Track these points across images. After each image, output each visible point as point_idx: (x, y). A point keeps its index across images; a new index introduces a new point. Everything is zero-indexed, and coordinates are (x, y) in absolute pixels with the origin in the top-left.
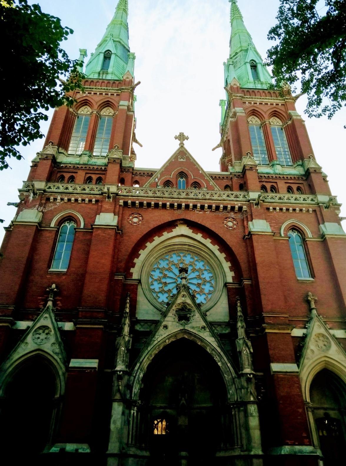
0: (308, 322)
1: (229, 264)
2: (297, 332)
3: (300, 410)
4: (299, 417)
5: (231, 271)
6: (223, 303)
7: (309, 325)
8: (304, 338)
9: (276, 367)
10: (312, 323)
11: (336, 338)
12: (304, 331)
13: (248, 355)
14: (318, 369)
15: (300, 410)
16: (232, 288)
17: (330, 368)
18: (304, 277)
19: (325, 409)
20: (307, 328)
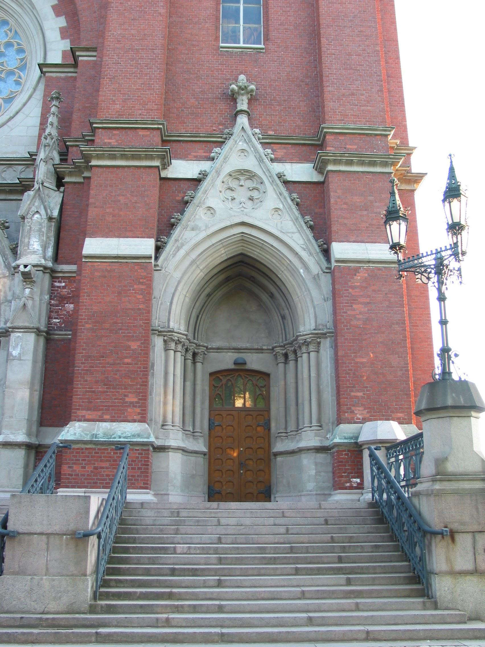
0: (221, 144)
1: (62, 22)
2: (182, 169)
3: (134, 345)
4: (126, 360)
5: (63, 38)
6: (31, 115)
7: (217, 150)
8: (196, 182)
9: (93, 246)
10: (230, 143)
11: (286, 183)
12: (205, 166)
13: (40, 224)
14: (222, 255)
15: (134, 345)
16: (57, 77)
17: (255, 253)
18: (244, 43)
19: (237, 350)
20: (213, 159)
